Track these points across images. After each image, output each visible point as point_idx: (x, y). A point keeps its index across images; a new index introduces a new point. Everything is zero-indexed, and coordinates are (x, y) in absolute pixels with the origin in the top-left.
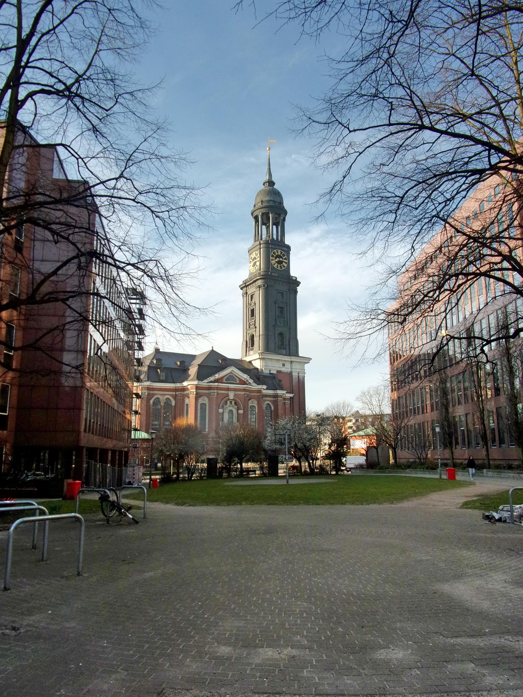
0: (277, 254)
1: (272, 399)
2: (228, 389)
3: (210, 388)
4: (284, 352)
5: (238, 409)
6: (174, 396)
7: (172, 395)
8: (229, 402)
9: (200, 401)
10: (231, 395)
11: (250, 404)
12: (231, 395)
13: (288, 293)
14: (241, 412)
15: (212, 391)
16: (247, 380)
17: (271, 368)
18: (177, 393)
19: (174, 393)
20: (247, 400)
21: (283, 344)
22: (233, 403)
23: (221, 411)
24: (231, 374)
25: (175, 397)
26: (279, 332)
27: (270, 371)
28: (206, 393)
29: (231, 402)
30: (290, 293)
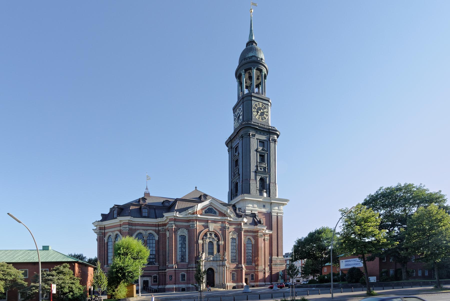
0: (258, 106)
6: (157, 231)
7: (155, 231)
9: (179, 233)
18: (160, 228)
19: (157, 228)
24: (211, 207)
25: (158, 232)
28: (185, 226)
29: (211, 234)
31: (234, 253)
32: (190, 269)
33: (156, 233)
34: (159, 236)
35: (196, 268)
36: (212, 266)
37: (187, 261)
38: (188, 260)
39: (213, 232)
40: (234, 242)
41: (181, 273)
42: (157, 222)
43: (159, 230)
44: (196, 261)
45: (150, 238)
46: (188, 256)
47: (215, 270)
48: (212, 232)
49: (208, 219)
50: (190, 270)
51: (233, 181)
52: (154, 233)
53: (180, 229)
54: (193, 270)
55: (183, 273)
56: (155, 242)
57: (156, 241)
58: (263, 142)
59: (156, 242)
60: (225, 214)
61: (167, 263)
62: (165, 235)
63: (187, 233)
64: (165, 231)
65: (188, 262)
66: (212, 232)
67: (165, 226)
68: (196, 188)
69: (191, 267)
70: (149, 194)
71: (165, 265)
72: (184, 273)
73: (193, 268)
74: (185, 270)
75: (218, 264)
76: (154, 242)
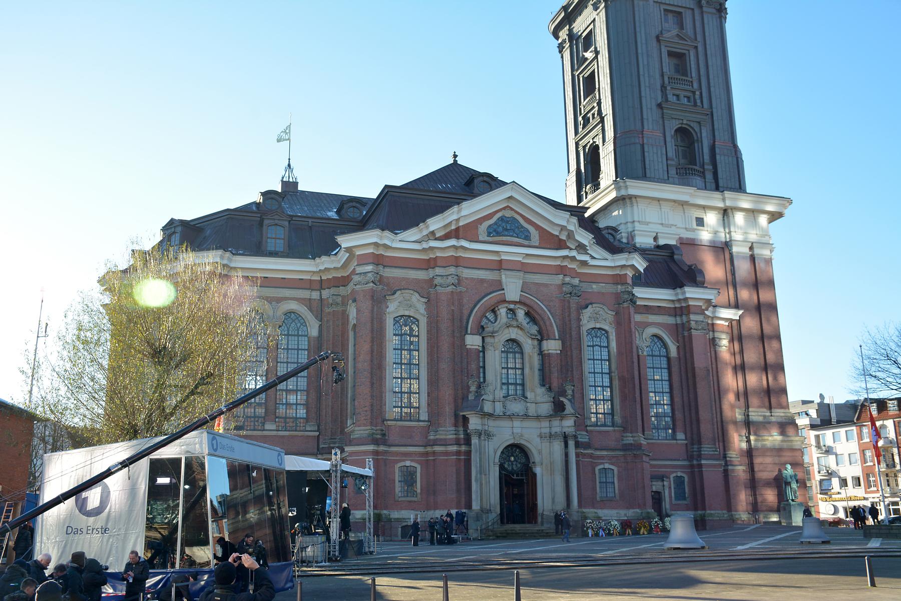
1: (670, 320)
2: (500, 265)
3: (430, 264)
4: (698, 180)
5: (542, 336)
7: (308, 303)
8: (502, 311)
10: (513, 288)
11: (587, 324)
12: (513, 288)
13: (697, 12)
14: (553, 346)
15: (438, 271)
16: (570, 235)
17: (659, 229)
18: (326, 293)
19: (315, 295)
20: (573, 306)
21: (693, 161)
22: (521, 313)
23: (473, 341)
24: (508, 214)
25: (318, 309)
26: (676, 125)
27: (655, 239)
28: (418, 281)
30: (702, 13)
31: (603, 387)
32: (438, 449)
33: (310, 309)
34: (321, 321)
35: (457, 442)
36: (522, 435)
37: (424, 416)
38: (428, 412)
39: (520, 302)
40: (600, 347)
41: (402, 464)
42: (314, 272)
43: (321, 299)
44: (456, 416)
45: (288, 330)
46: (428, 396)
47: (536, 457)
48: (518, 306)
49: (500, 256)
50: (434, 453)
51: (582, 143)
52: (303, 310)
53: (398, 293)
54: (446, 453)
55: (408, 463)
56: (306, 343)
57: (309, 341)
58: (680, 13)
59: (312, 343)
60: (563, 237)
61: (349, 422)
62: (345, 316)
63: (422, 308)
64: (344, 303)
65: (427, 419)
66: (515, 303)
67: (344, 286)
68: (455, 156)
69: (441, 439)
70: (295, 184)
71: (342, 432)
72: (413, 464)
73: (445, 443)
74: (415, 454)
75: (544, 431)
76: (304, 344)
